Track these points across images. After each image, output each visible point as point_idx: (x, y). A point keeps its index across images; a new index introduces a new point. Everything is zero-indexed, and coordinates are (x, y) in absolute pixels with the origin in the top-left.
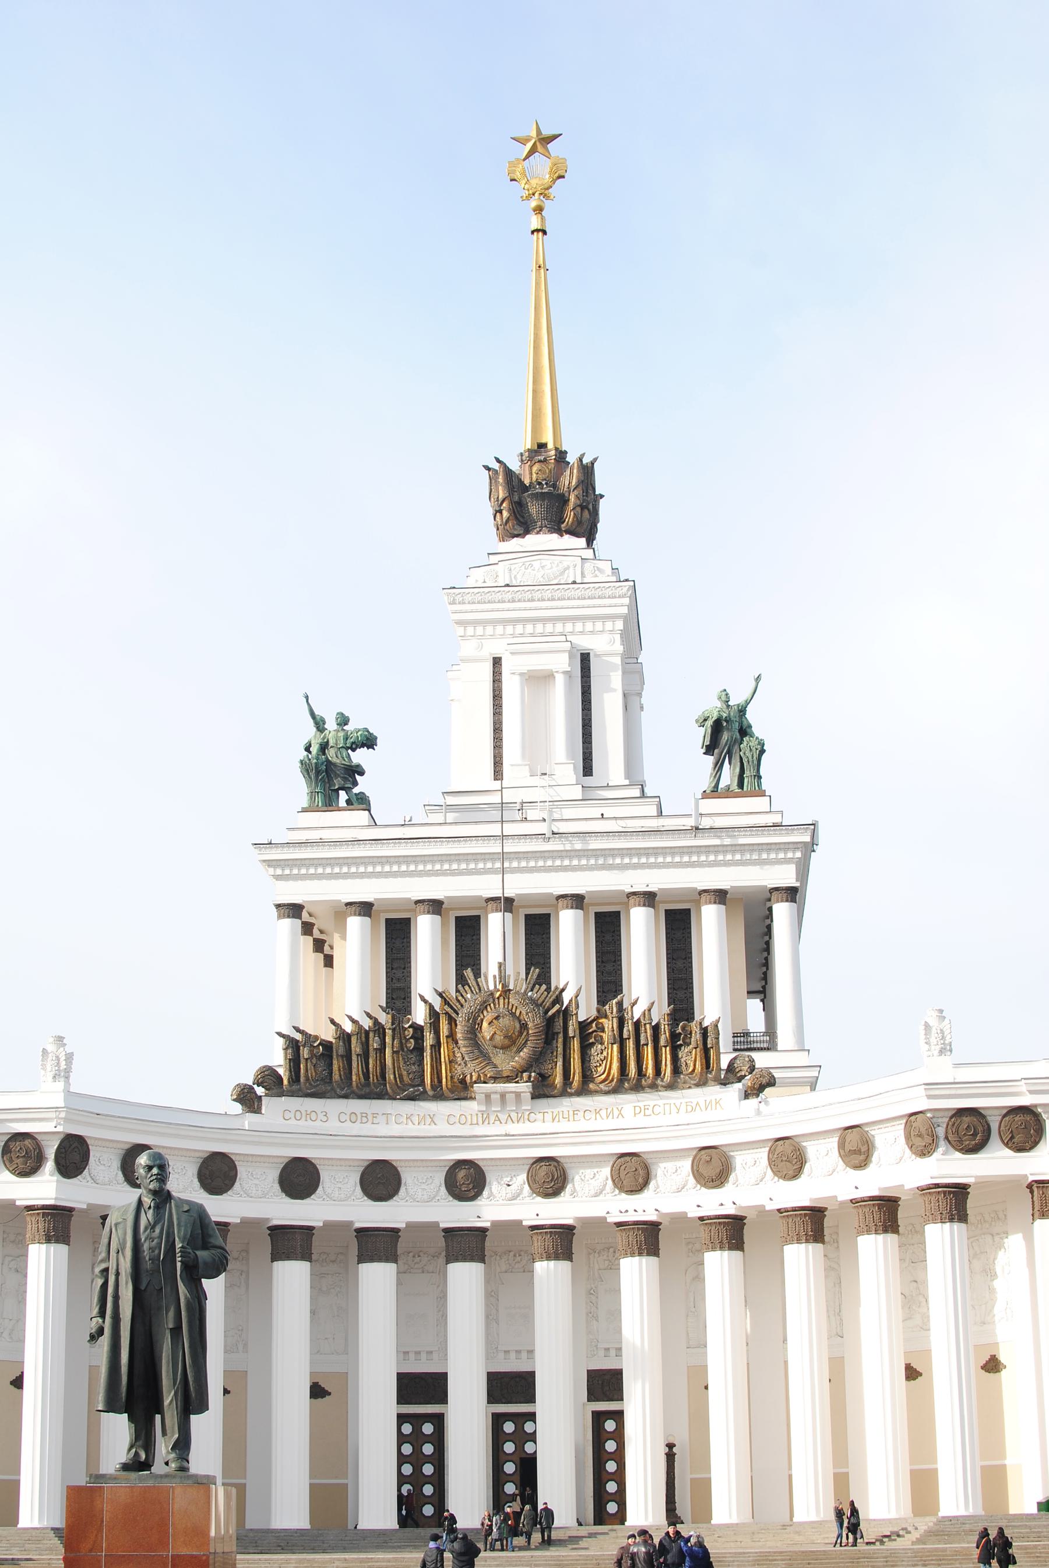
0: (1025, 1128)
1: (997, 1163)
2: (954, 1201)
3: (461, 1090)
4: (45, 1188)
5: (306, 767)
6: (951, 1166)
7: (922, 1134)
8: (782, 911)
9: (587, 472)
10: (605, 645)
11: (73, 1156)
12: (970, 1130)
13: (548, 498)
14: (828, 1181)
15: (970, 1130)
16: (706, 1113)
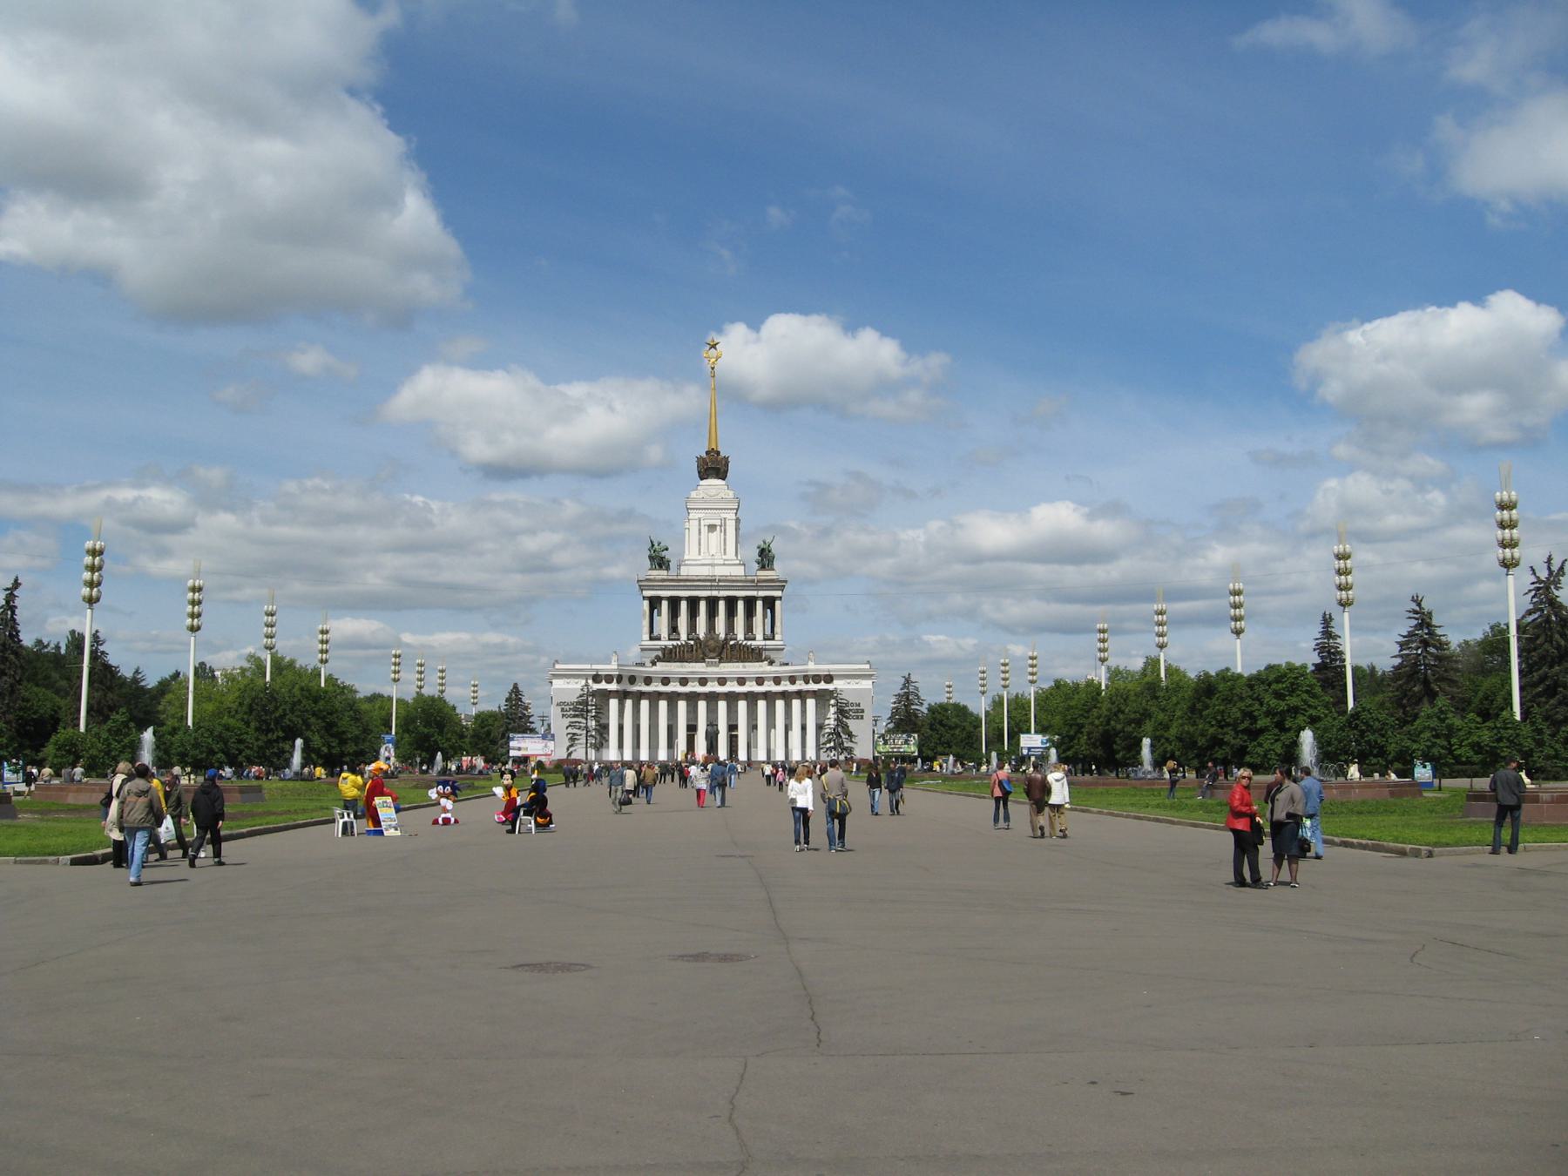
0: (829, 679)
1: (822, 686)
2: (814, 694)
3: (703, 660)
4: (613, 686)
5: (651, 557)
6: (813, 686)
7: (806, 679)
8: (778, 603)
9: (726, 460)
10: (731, 516)
11: (620, 679)
12: (816, 679)
13: (713, 467)
14: (785, 686)
15: (816, 679)
16: (761, 668)
